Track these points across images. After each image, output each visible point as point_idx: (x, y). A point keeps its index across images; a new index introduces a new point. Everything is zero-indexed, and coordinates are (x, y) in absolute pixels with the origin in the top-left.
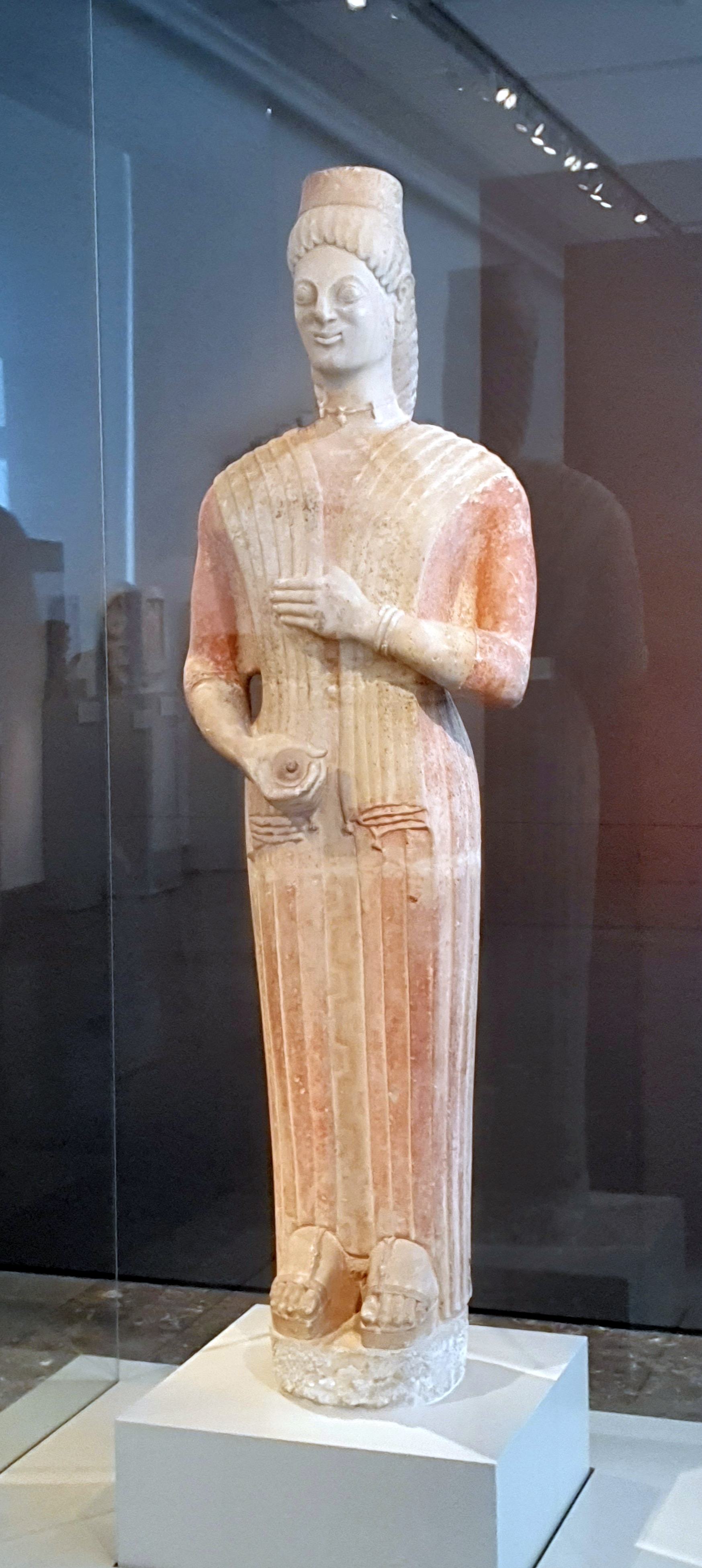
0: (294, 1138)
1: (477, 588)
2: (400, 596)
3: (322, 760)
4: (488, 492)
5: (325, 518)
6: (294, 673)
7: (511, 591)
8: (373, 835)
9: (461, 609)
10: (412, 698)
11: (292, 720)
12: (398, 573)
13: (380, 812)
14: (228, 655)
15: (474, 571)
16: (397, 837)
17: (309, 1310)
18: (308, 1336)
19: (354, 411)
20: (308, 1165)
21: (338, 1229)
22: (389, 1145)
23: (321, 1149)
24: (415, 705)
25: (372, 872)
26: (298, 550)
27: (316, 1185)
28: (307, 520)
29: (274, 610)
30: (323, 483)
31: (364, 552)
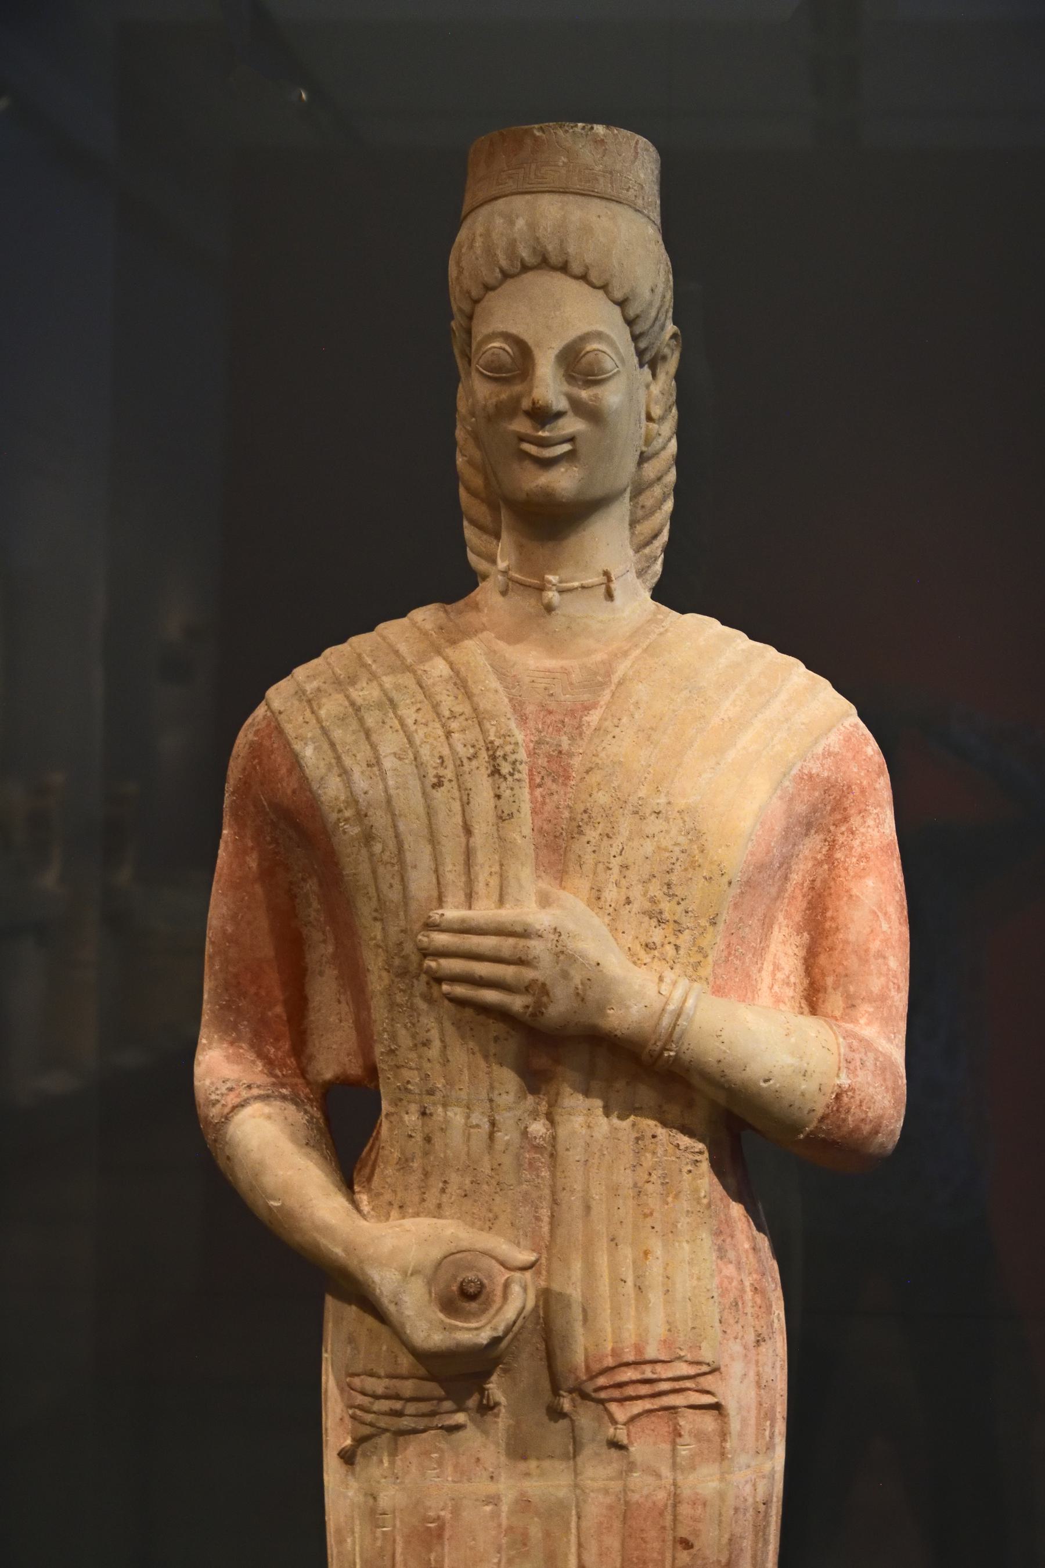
1: (805, 934)
2: (682, 952)
3: (528, 1275)
4: (830, 754)
5: (531, 794)
6: (463, 1095)
7: (875, 945)
8: (614, 1421)
9: (773, 974)
10: (701, 1153)
11: (453, 1189)
12: (680, 909)
13: (630, 1374)
14: (286, 1046)
15: (801, 904)
16: (660, 1425)
19: (576, 584)
24: (705, 1166)
25: (606, 1492)
26: (480, 857)
28: (498, 797)
29: (429, 972)
30: (523, 719)
31: (615, 863)
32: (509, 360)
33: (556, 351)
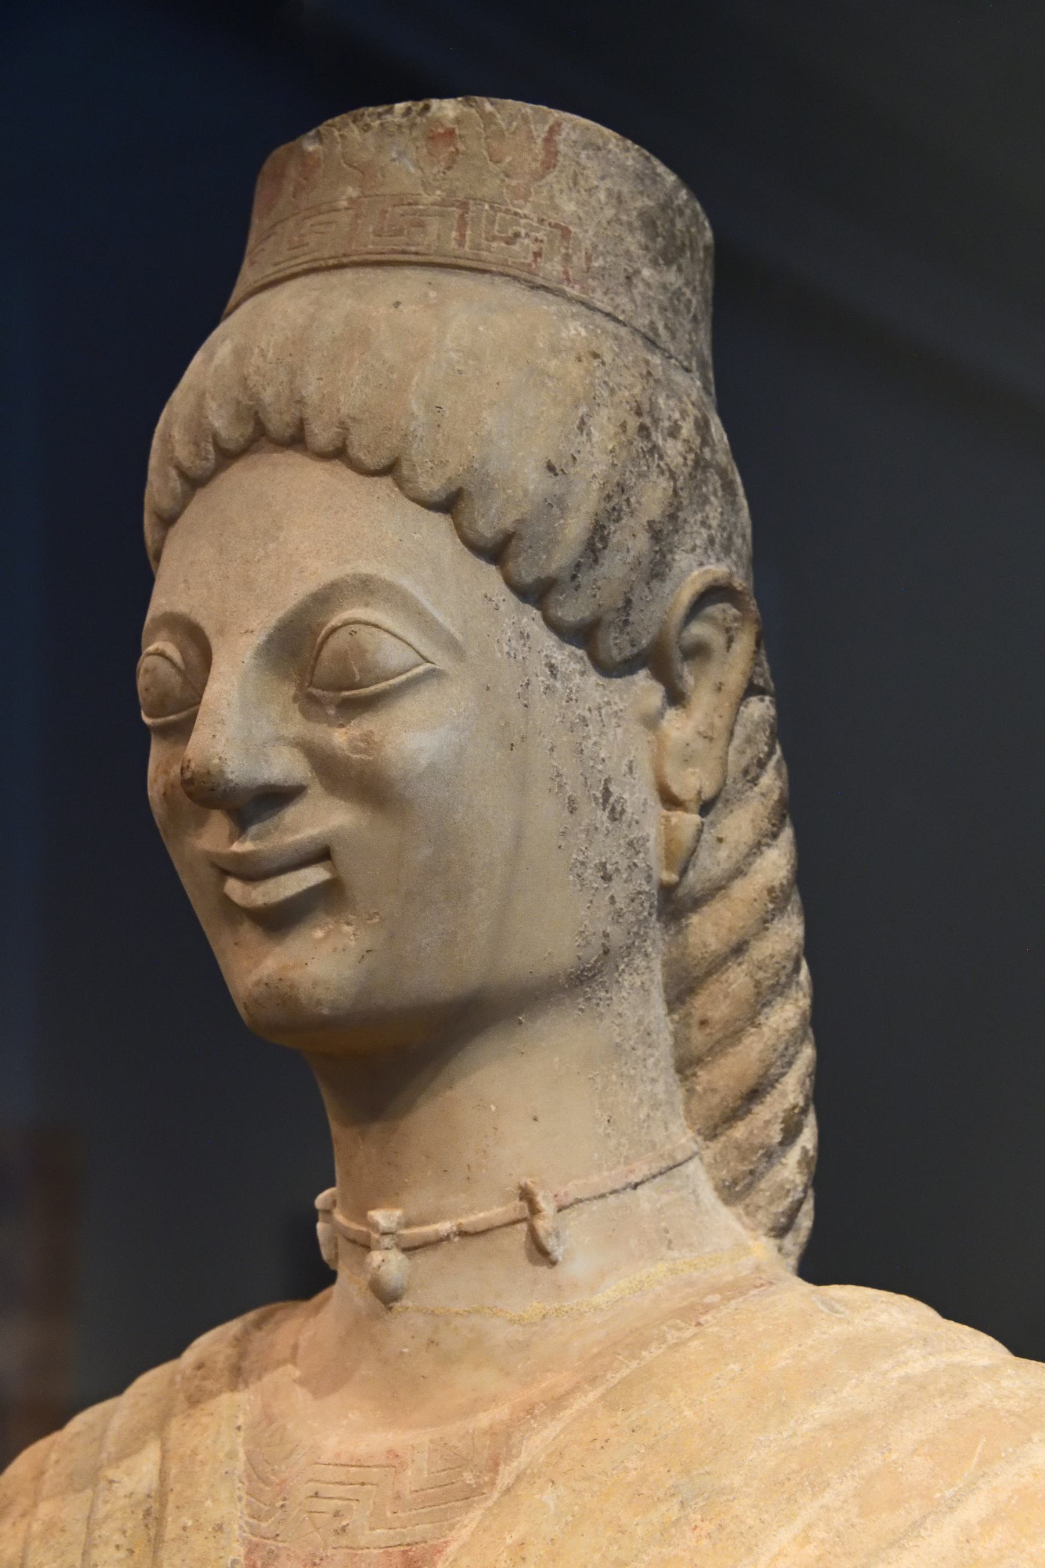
19: (445, 1227)
32: (176, 680)
33: (259, 639)
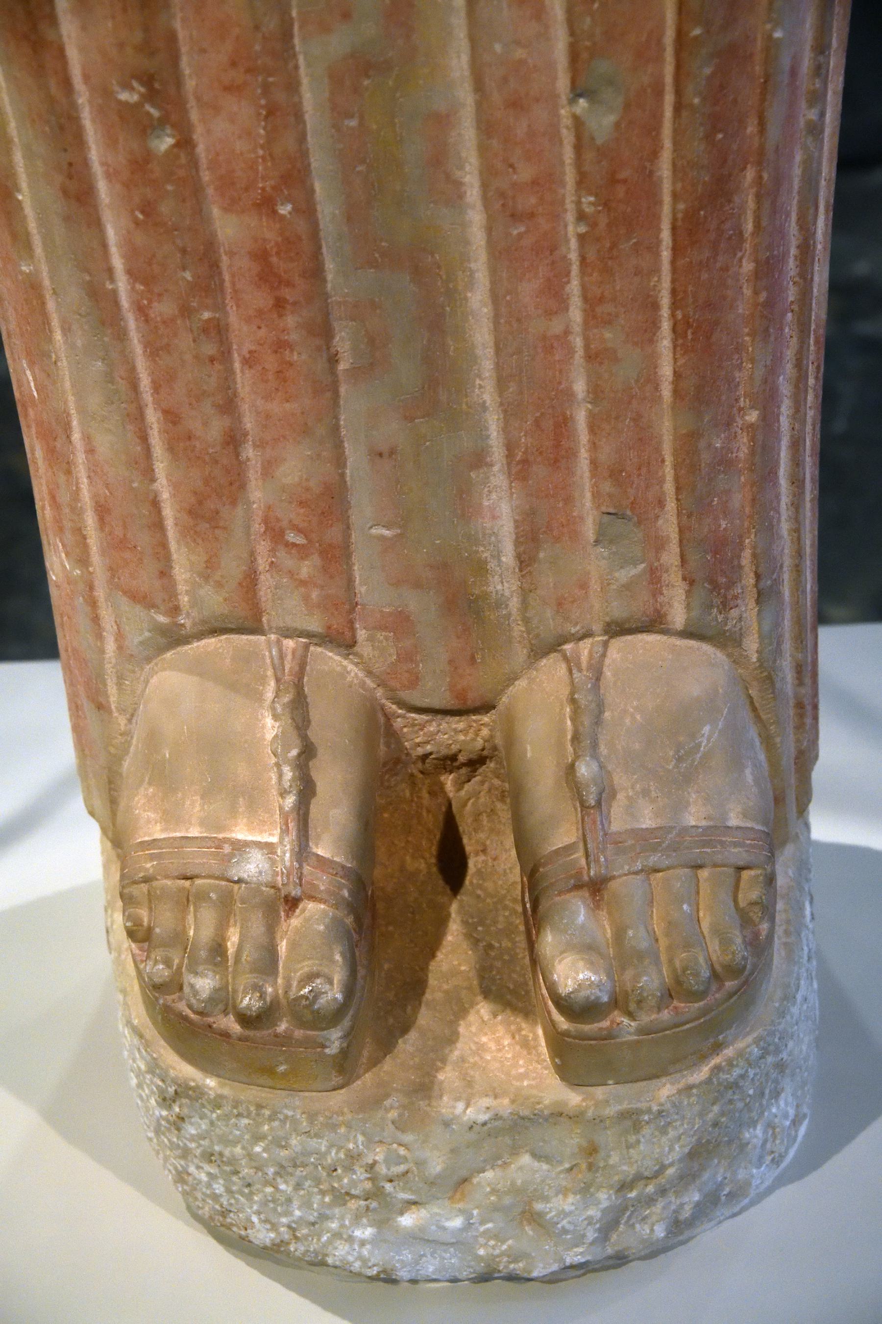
0: (131, 322)
17: (333, 993)
18: (336, 1080)
20: (215, 429)
21: (362, 634)
22: (576, 314)
23: (270, 362)
27: (257, 494)
